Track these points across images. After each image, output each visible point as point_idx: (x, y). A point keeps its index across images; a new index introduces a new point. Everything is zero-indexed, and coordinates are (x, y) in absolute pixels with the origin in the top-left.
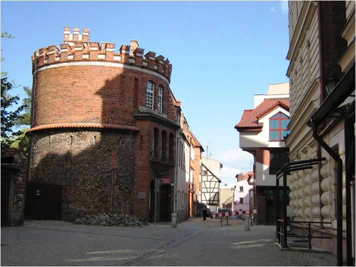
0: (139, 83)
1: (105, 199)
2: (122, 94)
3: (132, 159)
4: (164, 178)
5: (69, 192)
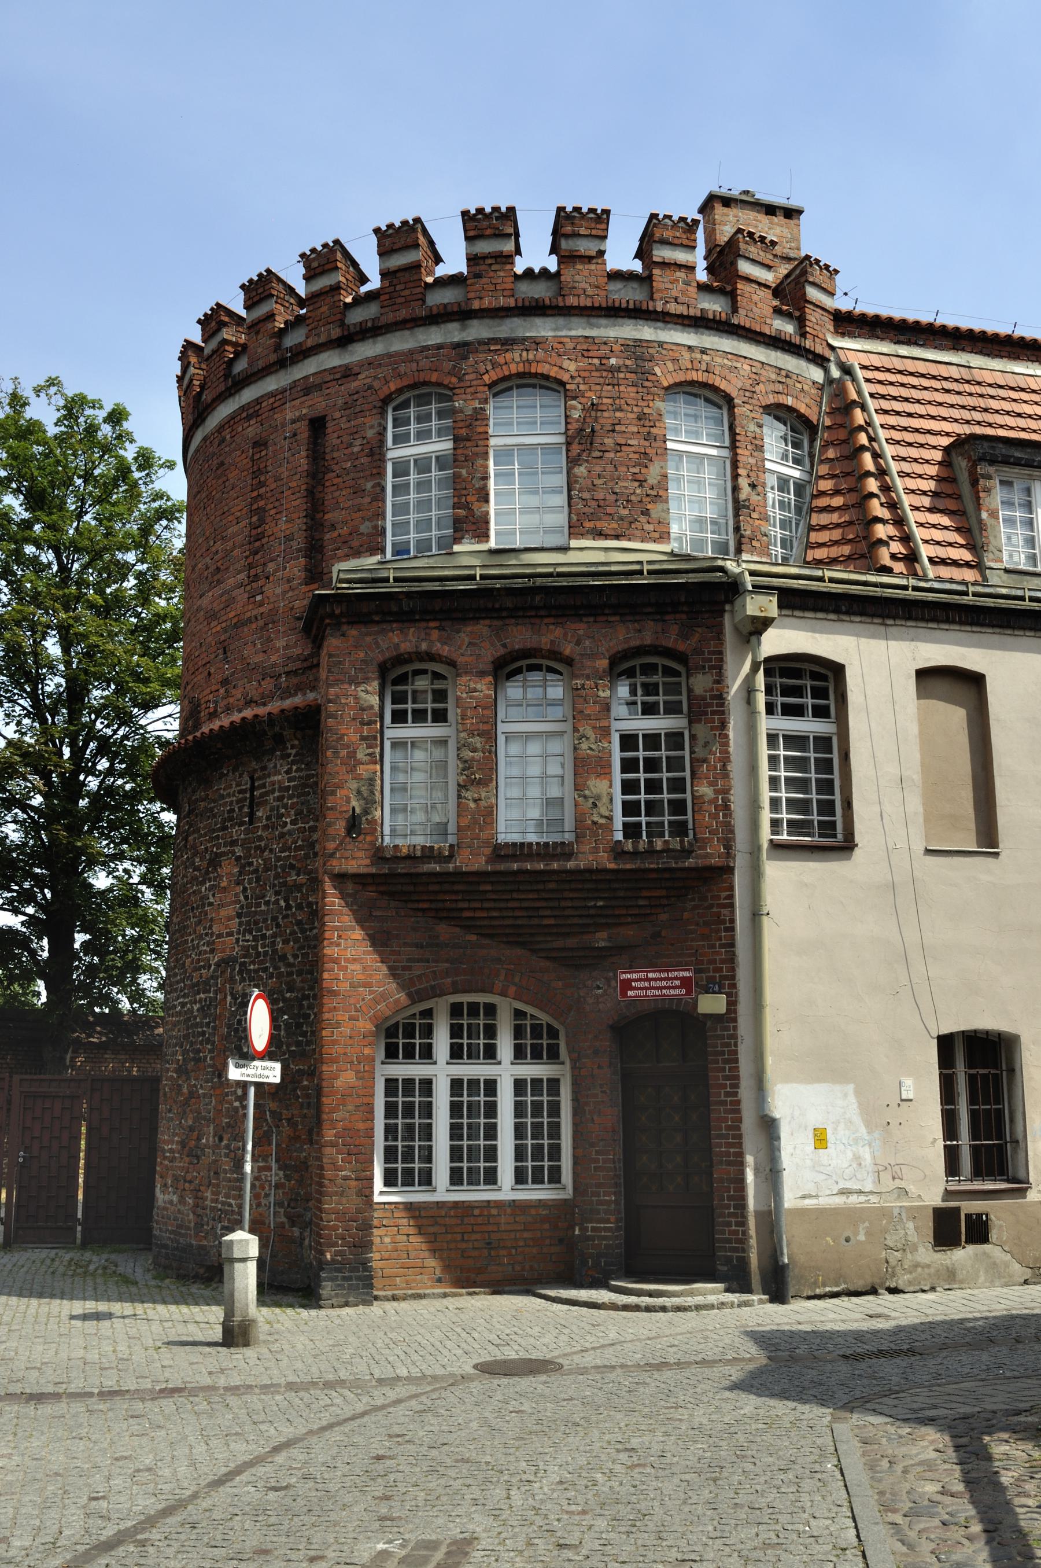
2: (257, 540)
3: (298, 887)
4: (631, 967)
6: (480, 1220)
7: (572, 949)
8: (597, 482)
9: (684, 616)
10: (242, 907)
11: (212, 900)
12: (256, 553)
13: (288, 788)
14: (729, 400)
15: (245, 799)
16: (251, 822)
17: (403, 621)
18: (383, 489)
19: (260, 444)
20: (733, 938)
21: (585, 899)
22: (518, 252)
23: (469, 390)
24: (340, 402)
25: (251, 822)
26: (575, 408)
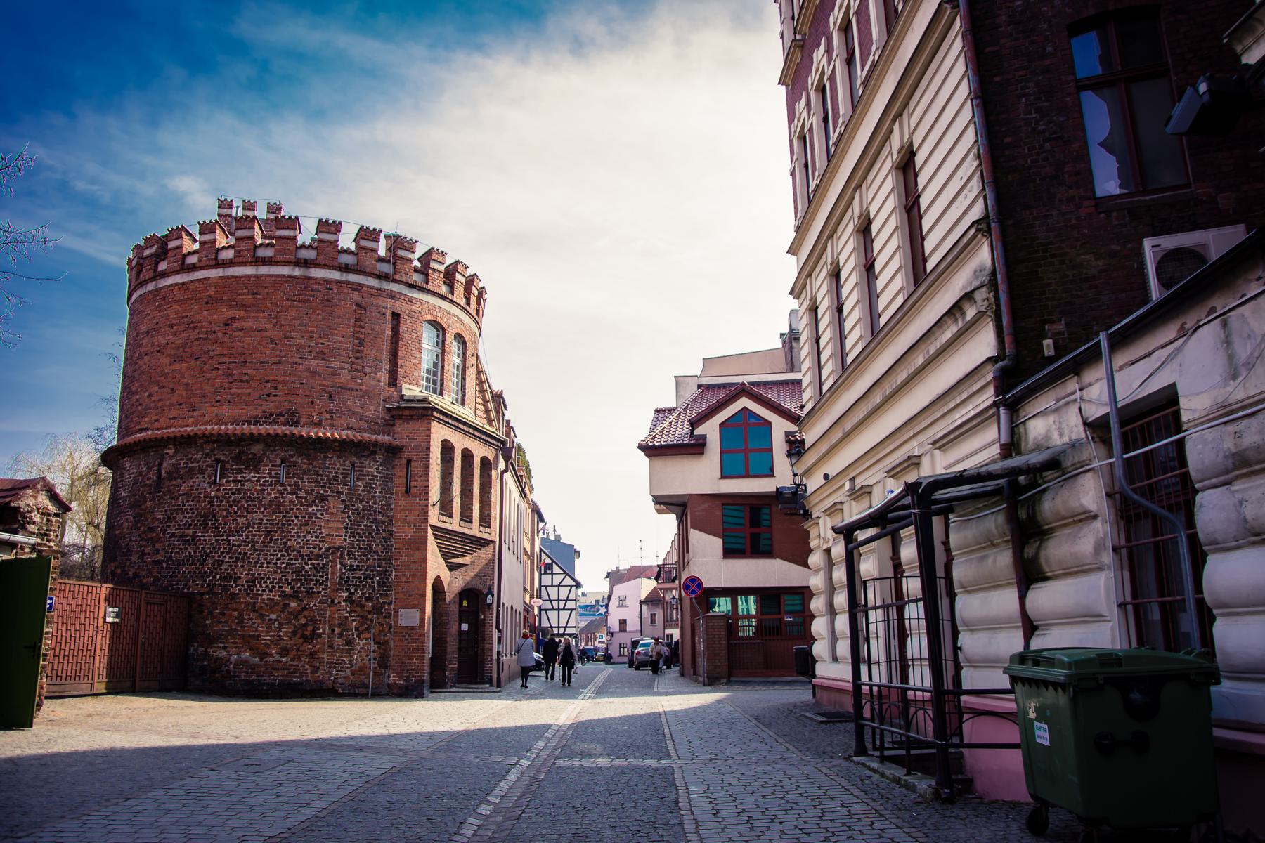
0: (402, 326)
1: (310, 628)
3: (384, 522)
5: (211, 613)
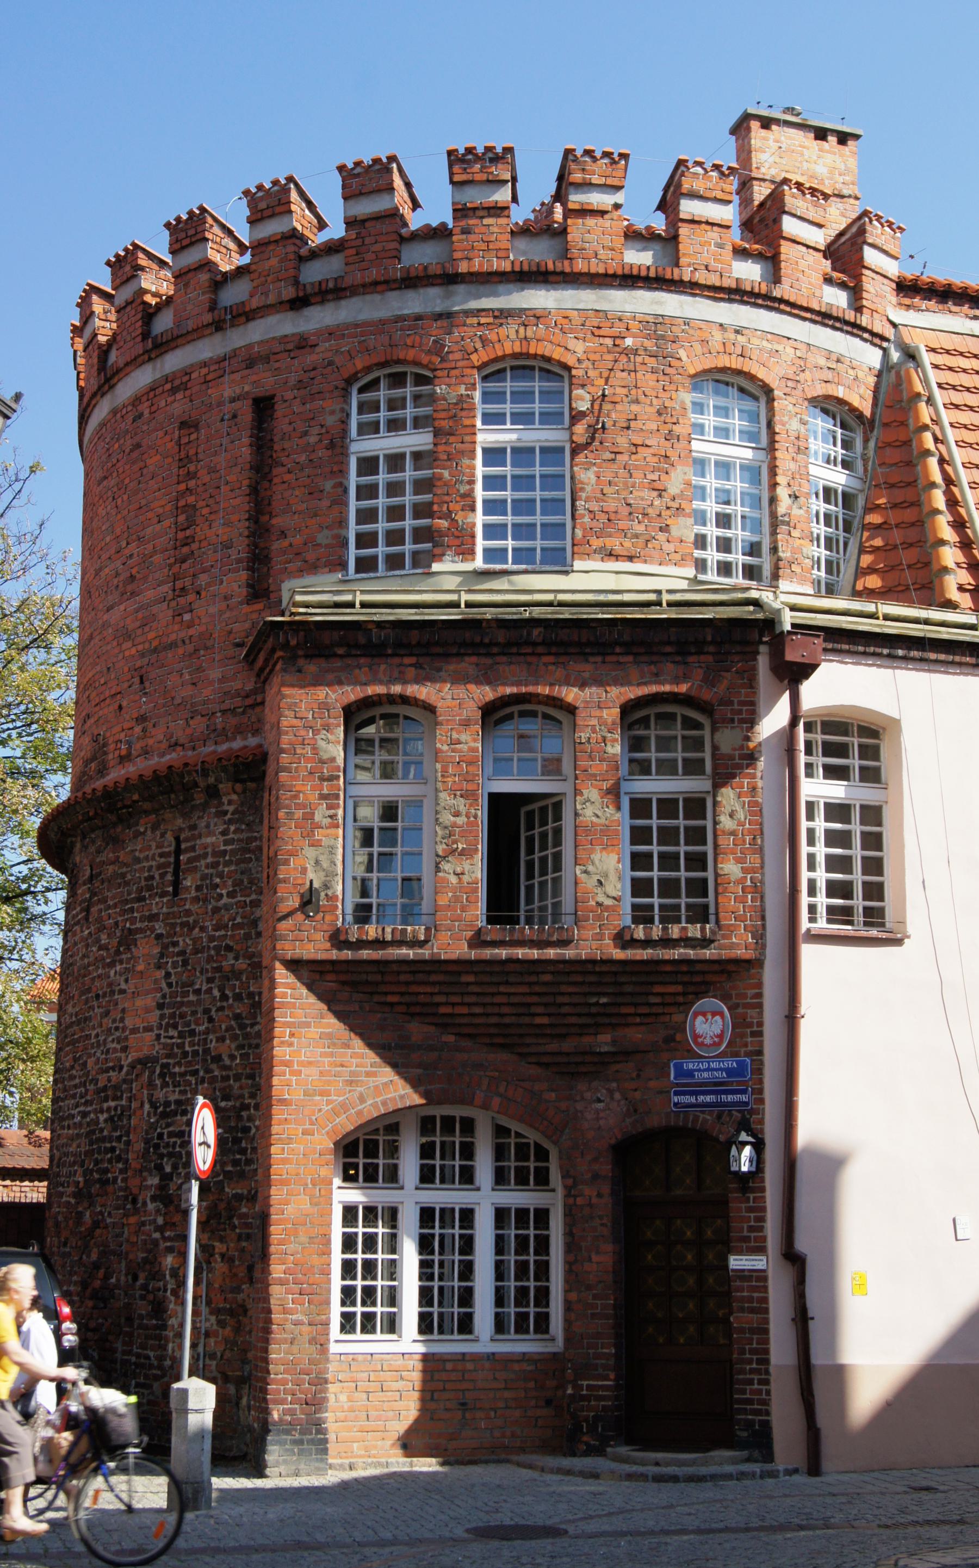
3: (237, 974)
6: (453, 1376)
7: (568, 1054)
8: (607, 490)
9: (710, 658)
10: (164, 996)
11: (123, 986)
12: (183, 561)
13: (224, 853)
14: (768, 391)
15: (169, 864)
16: (176, 893)
17: (373, 656)
18: (346, 490)
19: (188, 425)
20: (761, 1044)
21: (585, 994)
22: (515, 199)
23: (453, 372)
24: (292, 382)
25: (176, 893)
26: (582, 399)
